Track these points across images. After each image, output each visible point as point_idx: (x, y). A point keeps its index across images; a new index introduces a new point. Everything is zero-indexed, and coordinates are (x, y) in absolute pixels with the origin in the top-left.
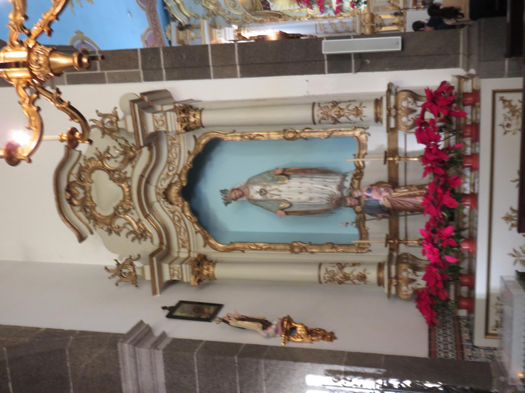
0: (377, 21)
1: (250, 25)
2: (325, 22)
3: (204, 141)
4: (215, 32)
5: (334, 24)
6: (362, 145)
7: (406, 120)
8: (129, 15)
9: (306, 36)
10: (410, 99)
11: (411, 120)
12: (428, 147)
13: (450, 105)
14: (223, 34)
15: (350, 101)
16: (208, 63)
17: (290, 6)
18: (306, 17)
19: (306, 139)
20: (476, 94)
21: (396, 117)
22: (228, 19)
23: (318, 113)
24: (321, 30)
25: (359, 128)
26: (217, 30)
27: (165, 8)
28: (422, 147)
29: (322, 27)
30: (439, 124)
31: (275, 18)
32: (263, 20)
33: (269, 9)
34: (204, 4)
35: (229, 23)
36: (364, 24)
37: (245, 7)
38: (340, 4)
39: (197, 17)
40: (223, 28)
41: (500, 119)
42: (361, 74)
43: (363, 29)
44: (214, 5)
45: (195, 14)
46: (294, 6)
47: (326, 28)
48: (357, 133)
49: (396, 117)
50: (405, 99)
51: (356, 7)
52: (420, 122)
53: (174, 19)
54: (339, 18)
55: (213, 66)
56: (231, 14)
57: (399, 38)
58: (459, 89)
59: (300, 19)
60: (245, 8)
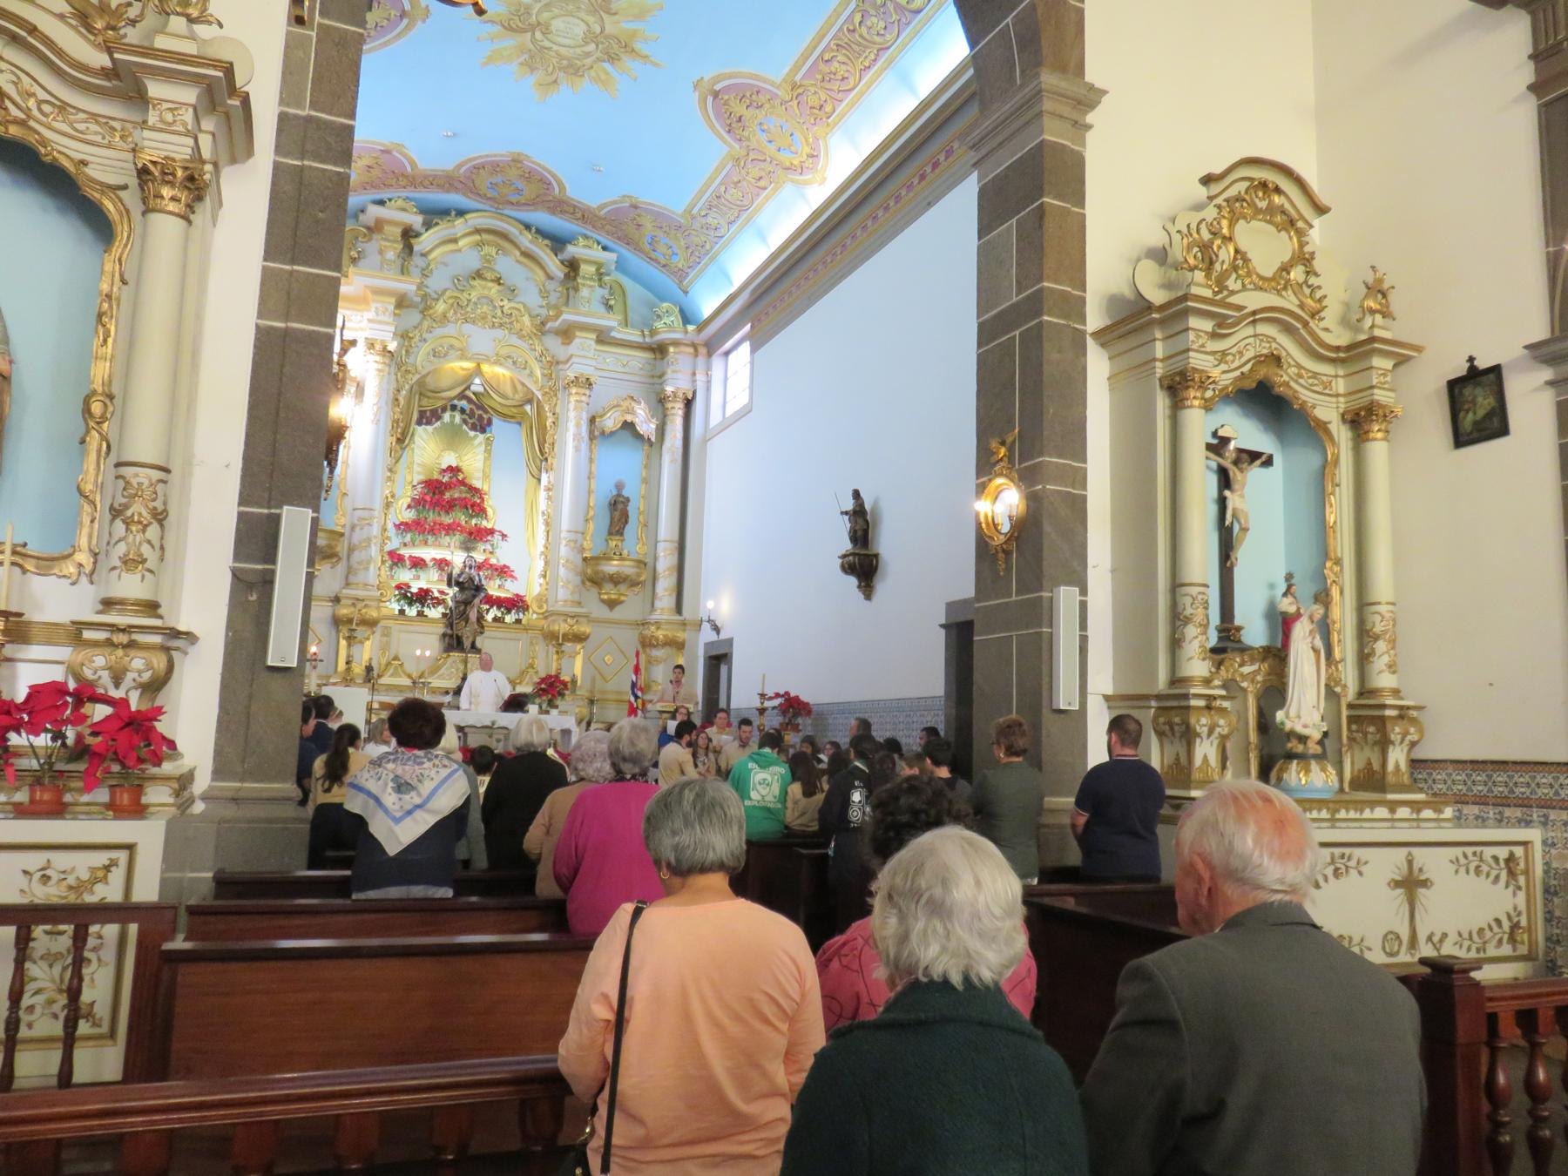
0: (361, 632)
1: (394, 377)
2: (375, 530)
3: (108, 205)
4: (389, 303)
5: (369, 546)
6: (47, 563)
7: (97, 666)
9: (331, 478)
10: (146, 676)
11: (96, 677)
12: (19, 708)
13: (117, 760)
14: (382, 318)
15: (162, 548)
16: (299, 265)
17: (422, 465)
19: (83, 442)
20: (138, 811)
21: (109, 643)
22: (411, 335)
23: (143, 476)
24: (360, 519)
25: (95, 563)
26: (391, 307)
27: (453, 213)
28: (21, 695)
30: (70, 733)
31: (399, 430)
33: (419, 423)
34: (448, 294)
35: (404, 336)
36: (360, 605)
38: (408, 562)
39: (425, 273)
41: (61, 860)
42: (228, 577)
43: (350, 602)
46: (419, 473)
48: (83, 557)
49: (109, 643)
50: (149, 667)
51: (397, 592)
52: (86, 693)
53: (428, 225)
54: (380, 558)
55: (292, 272)
56: (420, 344)
57: (295, 665)
58: (154, 778)
60: (428, 374)
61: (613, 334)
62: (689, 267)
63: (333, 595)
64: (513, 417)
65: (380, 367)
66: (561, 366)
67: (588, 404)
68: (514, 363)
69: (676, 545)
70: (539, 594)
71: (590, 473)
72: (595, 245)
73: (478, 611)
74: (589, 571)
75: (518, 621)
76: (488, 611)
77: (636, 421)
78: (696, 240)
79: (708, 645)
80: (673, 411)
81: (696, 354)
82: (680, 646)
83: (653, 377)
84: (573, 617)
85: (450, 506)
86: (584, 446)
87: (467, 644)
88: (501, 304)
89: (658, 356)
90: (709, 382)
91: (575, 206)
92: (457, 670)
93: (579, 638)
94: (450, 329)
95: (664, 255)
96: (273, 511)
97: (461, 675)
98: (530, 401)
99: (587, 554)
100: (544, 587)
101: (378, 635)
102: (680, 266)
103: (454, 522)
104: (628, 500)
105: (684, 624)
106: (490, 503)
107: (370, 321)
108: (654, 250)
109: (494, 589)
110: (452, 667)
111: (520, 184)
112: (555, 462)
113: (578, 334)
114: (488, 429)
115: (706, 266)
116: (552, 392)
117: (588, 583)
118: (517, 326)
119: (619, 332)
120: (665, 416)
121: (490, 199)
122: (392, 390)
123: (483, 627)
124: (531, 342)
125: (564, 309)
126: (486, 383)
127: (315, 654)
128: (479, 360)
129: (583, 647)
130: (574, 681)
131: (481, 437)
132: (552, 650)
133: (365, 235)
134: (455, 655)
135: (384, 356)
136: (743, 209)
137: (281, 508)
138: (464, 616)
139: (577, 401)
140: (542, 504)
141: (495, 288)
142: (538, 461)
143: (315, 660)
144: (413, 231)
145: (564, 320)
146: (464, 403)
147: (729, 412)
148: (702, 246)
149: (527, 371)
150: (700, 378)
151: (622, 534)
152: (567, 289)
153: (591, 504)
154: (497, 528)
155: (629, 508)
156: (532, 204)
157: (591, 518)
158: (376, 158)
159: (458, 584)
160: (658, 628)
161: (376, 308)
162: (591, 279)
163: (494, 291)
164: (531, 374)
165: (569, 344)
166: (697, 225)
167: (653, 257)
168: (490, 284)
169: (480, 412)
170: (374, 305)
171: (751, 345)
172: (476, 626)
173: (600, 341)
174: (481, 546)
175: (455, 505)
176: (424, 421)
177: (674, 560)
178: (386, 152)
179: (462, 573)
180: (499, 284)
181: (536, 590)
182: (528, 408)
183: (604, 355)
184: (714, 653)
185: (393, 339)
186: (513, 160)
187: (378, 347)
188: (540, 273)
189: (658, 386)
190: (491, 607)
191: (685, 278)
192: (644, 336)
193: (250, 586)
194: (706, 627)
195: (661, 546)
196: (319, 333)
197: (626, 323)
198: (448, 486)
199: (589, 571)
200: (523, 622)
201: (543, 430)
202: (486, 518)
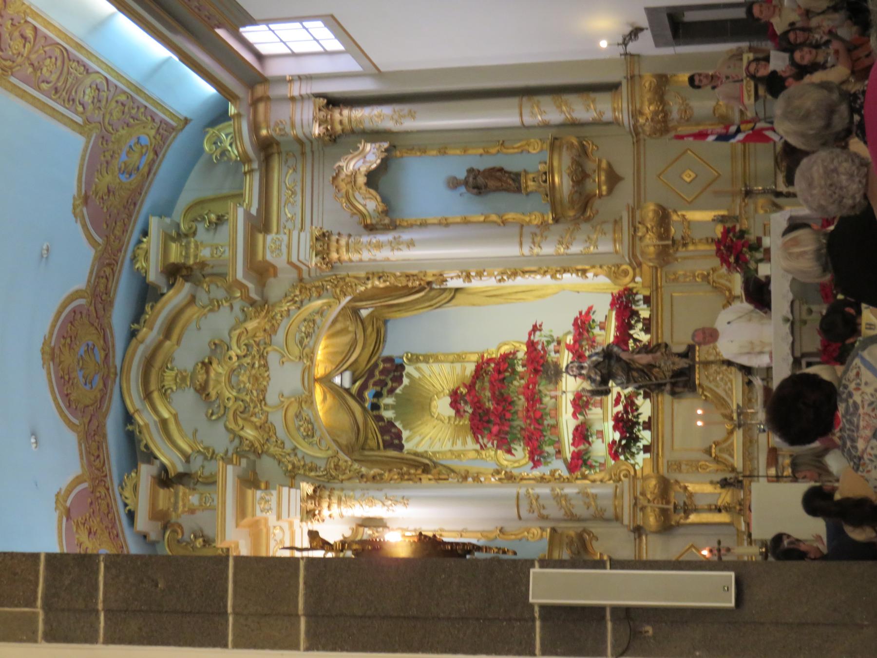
0: (676, 497)
1: (346, 484)
2: (544, 490)
4: (253, 496)
5: (566, 497)
8: (33, 440)
9: (487, 549)
14: (274, 503)
16: (226, 606)
18: (493, 475)
22: (290, 467)
24: (531, 510)
26: (259, 493)
27: (130, 427)
29: (534, 502)
31: (412, 471)
32: (381, 475)
33: (400, 447)
34: (232, 426)
35: (292, 477)
36: (642, 501)
37: (338, 440)
38: (582, 447)
39: (210, 456)
40: (275, 489)
43: (640, 515)
44: (259, 428)
45: (207, 448)
46: (464, 443)
47: (544, 508)
53: (150, 457)
54: (579, 482)
55: (235, 613)
56: (300, 455)
57: (732, 574)
59: (476, 479)
61: (254, 211)
62: (153, 120)
63: (632, 535)
64: (378, 332)
65: (335, 500)
66: (305, 275)
67: (350, 236)
68: (308, 335)
69: (525, 99)
70: (608, 276)
71: (440, 224)
72: (144, 246)
73: (639, 353)
74: (571, 213)
75: (647, 300)
76: (636, 340)
77: (364, 169)
78: (116, 114)
79: (659, 41)
80: (346, 120)
81: (266, 99)
82: (663, 81)
83: (303, 154)
84: (635, 230)
85: (504, 401)
86: (406, 236)
87: (683, 363)
88: (235, 359)
89: (275, 149)
90: (300, 78)
91: (98, 276)
92: (718, 373)
93: (663, 218)
94: (276, 419)
95: (142, 155)
96: (537, 615)
97: (725, 367)
98: (356, 312)
99: (550, 218)
100: (598, 270)
101: (679, 477)
102: (152, 133)
103: (524, 394)
104: (470, 171)
105: (631, 78)
106: (493, 349)
107: (279, 517)
108: (138, 169)
109: (608, 336)
110: (715, 380)
111: (83, 348)
112: (431, 272)
113: (260, 257)
114: (397, 361)
115: (148, 97)
116: (341, 284)
117: (588, 213)
118: (260, 335)
119: (250, 205)
120: (353, 132)
121: (105, 385)
122: (363, 485)
123: (658, 345)
124: (278, 317)
125: (230, 279)
126: (338, 369)
127: (711, 551)
128: (309, 379)
129: (675, 211)
130: (722, 220)
131: (409, 369)
132: (682, 252)
133: (174, 531)
134: (699, 377)
135: (321, 497)
136: (66, 56)
137: (532, 606)
138: (647, 371)
139: (348, 251)
140: (488, 283)
141: (217, 369)
142: (432, 294)
143: (719, 550)
144: (160, 475)
145: (245, 277)
146: (368, 395)
147: (335, 45)
148: (123, 105)
149: (317, 318)
150: (296, 90)
151: (518, 175)
152: (204, 276)
153: (482, 219)
154: (525, 339)
155: (482, 168)
156: (104, 331)
157: (501, 217)
158: (78, 526)
159: (604, 381)
160: (641, 113)
161: (262, 511)
162: (187, 247)
163: (220, 370)
164: (321, 312)
165: (274, 267)
166: (97, 116)
167: (146, 169)
168: (212, 375)
169: (377, 373)
170: (259, 514)
171: (244, 26)
172: (658, 354)
173: (266, 228)
174: (552, 356)
175: (502, 394)
176: (396, 442)
177: (546, 101)
178: (68, 513)
179: (589, 378)
180: (210, 363)
181: (603, 280)
182: (364, 313)
183: (283, 220)
184: (668, 33)
185: (299, 488)
186: (53, 359)
187: (310, 505)
188: (189, 312)
189: (315, 143)
190: (631, 336)
191: (167, 123)
192: (251, 171)
193: (635, 634)
194: (632, 47)
195: (528, 120)
196: (306, 577)
197: (238, 197)
198: (477, 405)
199: (571, 213)
200: (647, 293)
201: (392, 291)
202: (515, 353)
